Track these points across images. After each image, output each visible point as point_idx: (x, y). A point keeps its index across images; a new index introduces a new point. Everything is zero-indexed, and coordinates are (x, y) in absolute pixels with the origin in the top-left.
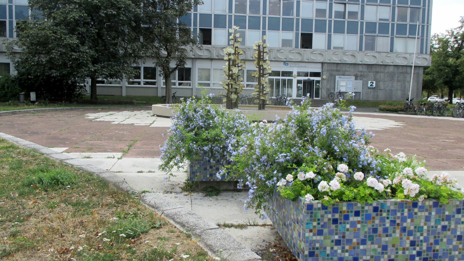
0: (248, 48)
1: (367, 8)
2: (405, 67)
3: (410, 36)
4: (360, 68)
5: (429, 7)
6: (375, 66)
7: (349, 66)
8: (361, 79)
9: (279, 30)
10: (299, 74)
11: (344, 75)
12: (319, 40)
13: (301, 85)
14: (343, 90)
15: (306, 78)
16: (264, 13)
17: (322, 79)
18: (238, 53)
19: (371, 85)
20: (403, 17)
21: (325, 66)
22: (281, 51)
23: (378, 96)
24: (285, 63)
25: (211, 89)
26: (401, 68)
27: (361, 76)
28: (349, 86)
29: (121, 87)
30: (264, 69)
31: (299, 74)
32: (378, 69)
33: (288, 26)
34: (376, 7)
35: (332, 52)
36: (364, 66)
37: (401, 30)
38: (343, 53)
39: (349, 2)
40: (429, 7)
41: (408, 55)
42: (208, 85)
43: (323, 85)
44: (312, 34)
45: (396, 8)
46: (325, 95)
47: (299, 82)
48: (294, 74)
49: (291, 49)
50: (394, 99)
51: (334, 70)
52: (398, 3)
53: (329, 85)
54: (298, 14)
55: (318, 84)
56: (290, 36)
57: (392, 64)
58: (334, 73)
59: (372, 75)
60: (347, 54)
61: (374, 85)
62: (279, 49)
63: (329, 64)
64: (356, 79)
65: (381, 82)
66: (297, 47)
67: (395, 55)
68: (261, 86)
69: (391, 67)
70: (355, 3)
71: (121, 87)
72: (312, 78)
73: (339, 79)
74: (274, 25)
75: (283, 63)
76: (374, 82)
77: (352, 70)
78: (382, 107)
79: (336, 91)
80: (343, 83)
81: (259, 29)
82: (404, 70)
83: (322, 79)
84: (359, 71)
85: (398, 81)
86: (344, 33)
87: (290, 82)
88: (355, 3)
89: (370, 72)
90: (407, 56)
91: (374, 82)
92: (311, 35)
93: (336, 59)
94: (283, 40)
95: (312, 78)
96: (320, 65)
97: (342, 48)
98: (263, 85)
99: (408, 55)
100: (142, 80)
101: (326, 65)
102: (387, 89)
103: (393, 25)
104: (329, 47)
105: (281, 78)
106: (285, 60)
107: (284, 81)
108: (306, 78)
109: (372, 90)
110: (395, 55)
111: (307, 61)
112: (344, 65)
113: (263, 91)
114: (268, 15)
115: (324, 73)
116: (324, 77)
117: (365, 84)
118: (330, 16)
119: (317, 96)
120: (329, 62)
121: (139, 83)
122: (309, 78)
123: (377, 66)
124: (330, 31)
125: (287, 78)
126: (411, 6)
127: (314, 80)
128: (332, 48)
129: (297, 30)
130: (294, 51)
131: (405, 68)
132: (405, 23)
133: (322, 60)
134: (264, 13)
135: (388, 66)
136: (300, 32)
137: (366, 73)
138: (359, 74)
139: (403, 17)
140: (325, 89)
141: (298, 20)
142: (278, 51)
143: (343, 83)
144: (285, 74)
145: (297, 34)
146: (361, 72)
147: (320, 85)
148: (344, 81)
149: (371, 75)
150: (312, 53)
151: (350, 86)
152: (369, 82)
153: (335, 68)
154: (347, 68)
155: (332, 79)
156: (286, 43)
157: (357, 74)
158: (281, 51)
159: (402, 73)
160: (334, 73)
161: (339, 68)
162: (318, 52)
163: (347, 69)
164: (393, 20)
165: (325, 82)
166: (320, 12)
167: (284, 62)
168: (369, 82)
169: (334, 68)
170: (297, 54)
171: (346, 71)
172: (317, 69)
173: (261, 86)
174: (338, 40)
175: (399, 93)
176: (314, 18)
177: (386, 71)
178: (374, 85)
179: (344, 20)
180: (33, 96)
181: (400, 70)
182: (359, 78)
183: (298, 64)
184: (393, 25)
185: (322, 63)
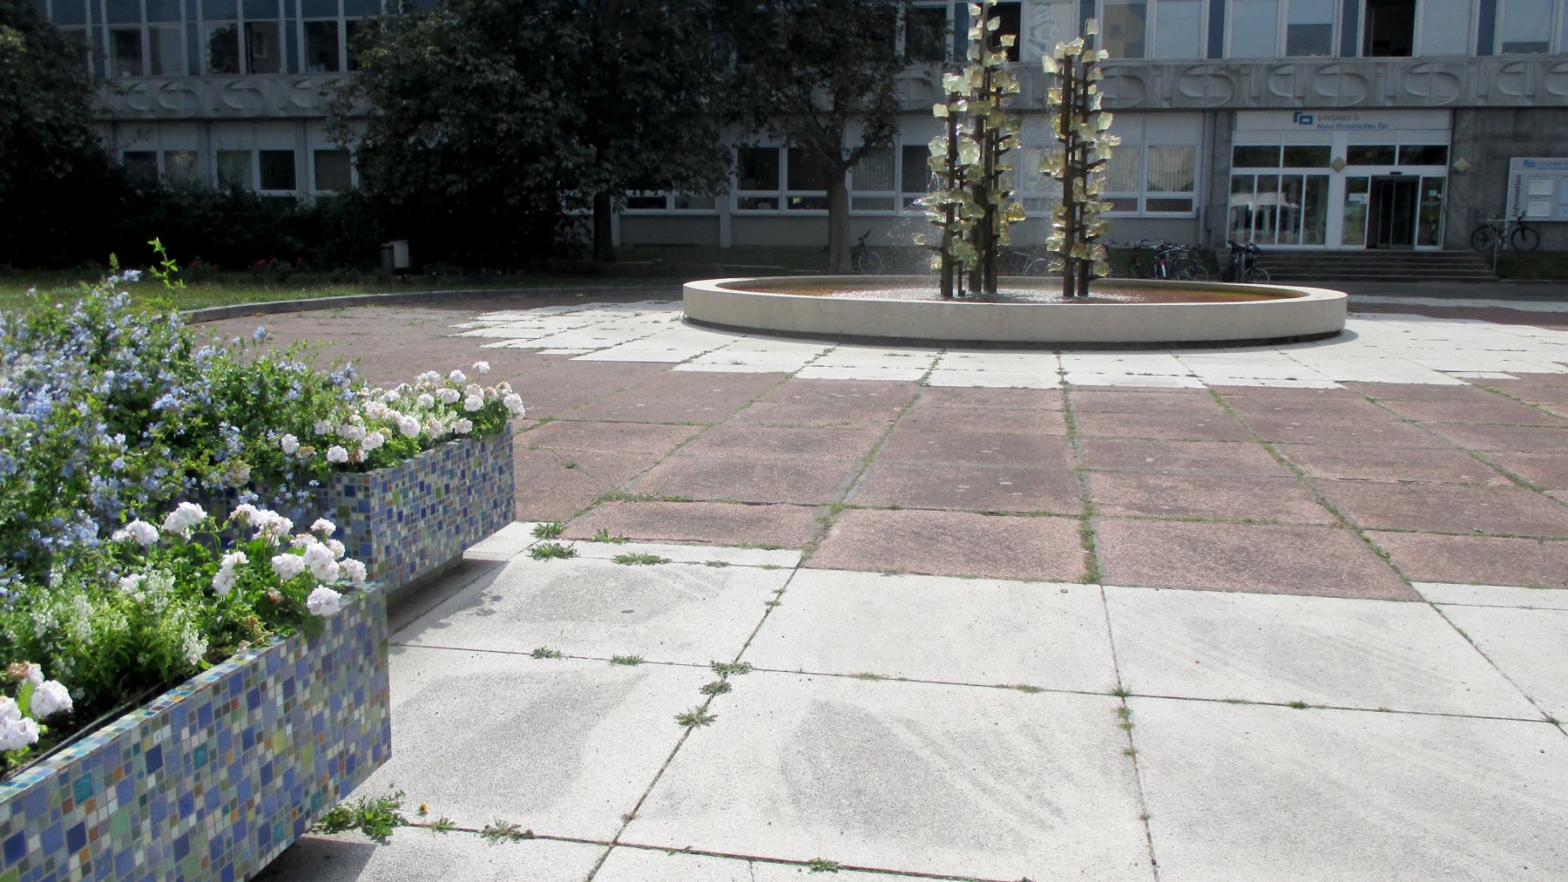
0: (1157, 67)
10: (1357, 155)
13: (1365, 198)
15: (1383, 171)
17: (1453, 172)
18: (999, 90)
21: (1466, 121)
22: (1284, 71)
24: (1301, 113)
29: (717, 218)
30: (1086, 148)
31: (1357, 155)
47: (1354, 185)
48: (1333, 157)
49: (1323, 59)
55: (1433, 193)
62: (1275, 63)
66: (1348, 50)
72: (1408, 170)
73: (1525, 172)
75: (1291, 115)
79: (1510, 216)
80: (1536, 188)
87: (1318, 188)
93: (1511, 92)
95: (1408, 170)
96: (1444, 120)
97: (1542, 47)
100: (783, 192)
101: (1472, 114)
104: (1485, 47)
106: (1298, 104)
108: (1383, 171)
111: (1389, 104)
113: (1083, 229)
116: (1461, 164)
120: (1481, 103)
121: (774, 203)
122: (1396, 168)
128: (1498, 50)
140: (1465, 211)
142: (1272, 69)
143: (1536, 188)
144: (1298, 156)
147: (1443, 196)
148: (1547, 177)
150: (1409, 71)
155: (1494, 167)
158: (1284, 71)
162: (1438, 69)
167: (1297, 111)
169: (1506, 126)
172: (1434, 132)
179: (351, 18)
180: (400, 253)
185: (1456, 111)
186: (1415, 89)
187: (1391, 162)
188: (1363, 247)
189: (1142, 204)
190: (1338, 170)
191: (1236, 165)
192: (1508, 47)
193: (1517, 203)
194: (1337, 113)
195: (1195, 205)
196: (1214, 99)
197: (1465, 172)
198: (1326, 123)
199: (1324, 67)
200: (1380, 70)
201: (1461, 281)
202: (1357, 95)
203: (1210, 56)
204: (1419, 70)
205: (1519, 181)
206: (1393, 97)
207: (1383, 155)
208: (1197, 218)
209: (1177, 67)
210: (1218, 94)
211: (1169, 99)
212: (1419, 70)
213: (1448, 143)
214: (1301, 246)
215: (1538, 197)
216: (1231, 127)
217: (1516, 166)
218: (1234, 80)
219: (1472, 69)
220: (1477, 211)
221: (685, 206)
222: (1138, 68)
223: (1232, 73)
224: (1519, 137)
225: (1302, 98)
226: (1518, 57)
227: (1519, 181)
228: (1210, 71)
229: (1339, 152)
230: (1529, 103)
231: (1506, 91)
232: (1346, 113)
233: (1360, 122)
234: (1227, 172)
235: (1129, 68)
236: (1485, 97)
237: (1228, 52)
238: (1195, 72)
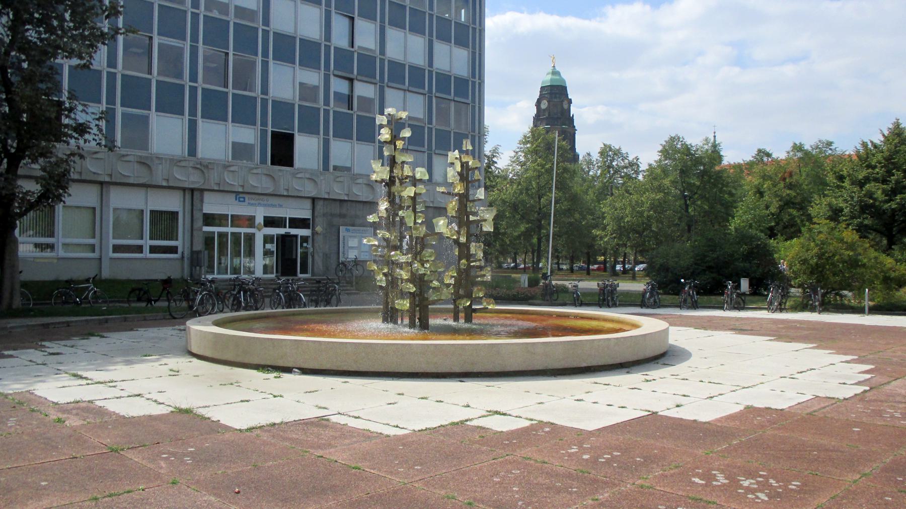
5: (479, 104)
9: (226, 120)
10: (270, 222)
11: (353, 225)
13: (272, 247)
16: (194, 78)
20: (443, 115)
21: (319, 205)
22: (232, 169)
24: (240, 195)
25: (59, 259)
31: (270, 222)
33: (244, 115)
34: (401, 93)
39: (359, 78)
40: (479, 104)
42: (51, 247)
43: (316, 245)
45: (434, 100)
47: (267, 239)
49: (250, 164)
52: (437, 91)
54: (265, 90)
55: (305, 245)
56: (247, 135)
60: (359, 181)
66: (263, 161)
70: (369, 80)
72: (294, 231)
73: (346, 234)
74: (214, 108)
75: (234, 195)
80: (353, 243)
81: (182, 114)
86: (352, 139)
87: (250, 238)
88: (369, 80)
92: (290, 138)
93: (339, 191)
94: (234, 144)
95: (294, 231)
96: (308, 204)
97: (348, 169)
103: (430, 129)
105: (229, 230)
106: (240, 190)
107: (236, 236)
108: (282, 231)
114: (201, 84)
115: (317, 220)
118: (327, 103)
119: (304, 270)
120: (326, 197)
124: (326, 132)
125: (243, 230)
126: (456, 99)
127: (296, 236)
129: (264, 123)
130: (259, 171)
132: (447, 129)
133: (312, 194)
134: (194, 78)
140: (321, 255)
141: (264, 102)
142: (226, 167)
144: (236, 220)
145: (264, 133)
148: (355, 237)
150: (294, 175)
153: (337, 211)
156: (240, 150)
158: (232, 169)
162: (308, 176)
165: (319, 239)
166: (307, 91)
167: (237, 193)
169: (336, 209)
170: (264, 178)
172: (304, 213)
174: (341, 151)
176: (297, 102)
184: (430, 129)
185: (314, 200)
187: (285, 227)
188: (273, 276)
189: (146, 249)
192: (336, 168)
194: (257, 197)
195: (180, 250)
196: (193, 182)
199: (252, 169)
202: (265, 185)
203: (189, 155)
204: (299, 176)
208: (183, 257)
209: (171, 160)
210: (193, 180)
211: (168, 180)
212: (299, 176)
213: (310, 217)
214: (229, 276)
215: (352, 248)
218: (205, 171)
222: (147, 158)
223: (204, 167)
224: (342, 216)
226: (338, 173)
228: (191, 165)
229: (260, 220)
230: (346, 198)
232: (261, 197)
233: (269, 203)
234: (201, 229)
235: (141, 157)
236: (329, 193)
237: (201, 153)
238: (183, 164)
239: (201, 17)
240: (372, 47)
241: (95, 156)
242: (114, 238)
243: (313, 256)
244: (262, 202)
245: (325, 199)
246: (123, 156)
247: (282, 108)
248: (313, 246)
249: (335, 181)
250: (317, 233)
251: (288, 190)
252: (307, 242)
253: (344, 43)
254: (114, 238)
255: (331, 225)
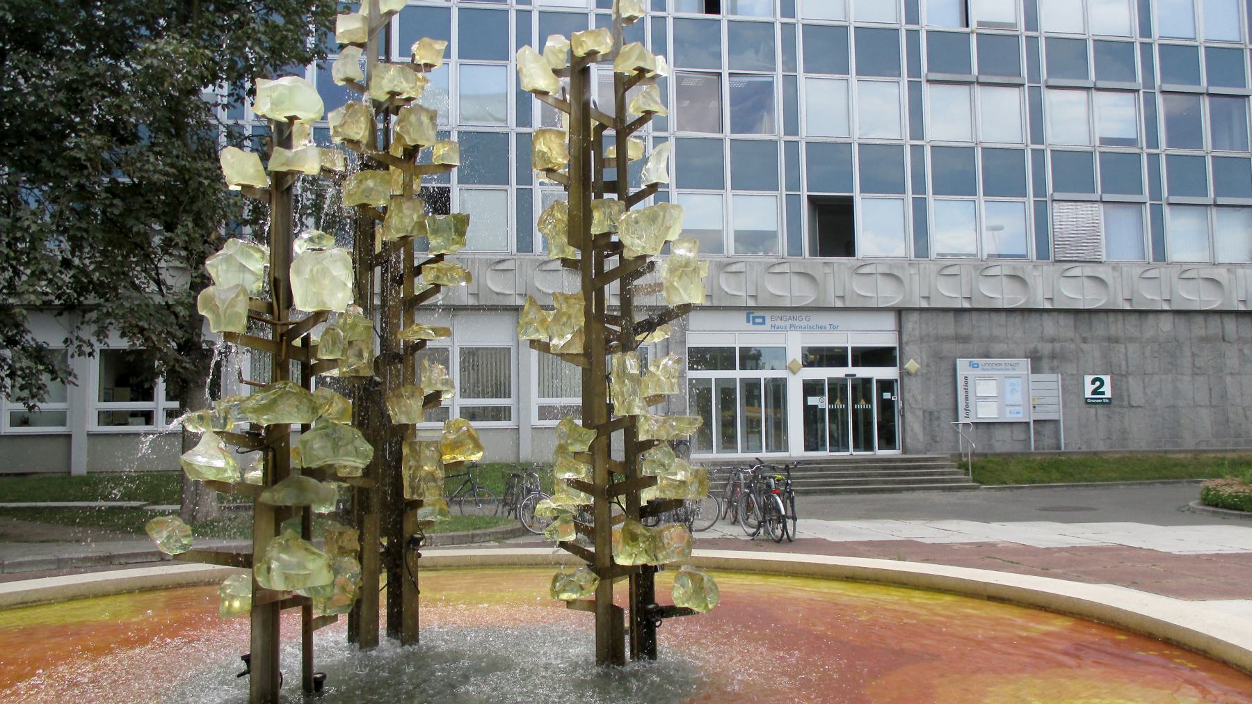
1: (1051, 99)
2: (1217, 318)
3: (1220, 201)
4: (1049, 326)
6: (1102, 316)
7: (1002, 318)
8: (1053, 370)
11: (987, 357)
12: (878, 225)
14: (987, 412)
15: (838, 372)
17: (904, 374)
19: (1094, 392)
20: (1183, 130)
21: (911, 322)
22: (734, 268)
23: (1124, 432)
24: (755, 312)
26: (1200, 320)
27: (1053, 356)
28: (1010, 399)
32: (1117, 327)
33: (755, 172)
34: (1082, 95)
35: (934, 268)
36: (1063, 320)
37: (1186, 177)
38: (976, 267)
41: (1223, 271)
43: (907, 395)
44: (851, 199)
45: (1160, 99)
46: (921, 436)
47: (811, 388)
50: (1189, 442)
51: (946, 339)
52: (1163, 80)
53: (932, 397)
54: (792, 125)
55: (887, 396)
57: (1166, 307)
58: (947, 348)
59: (1097, 354)
61: (1107, 390)
63: (925, 316)
64: (1036, 369)
65: (1130, 379)
66: (795, 249)
67: (1175, 271)
68: (618, 438)
69: (1163, 317)
71: (68, 437)
73: (971, 373)
75: (743, 315)
76: (1107, 379)
77: (1019, 334)
78: (1228, 487)
80: (985, 388)
82: (1214, 325)
83: (904, 374)
84: (1042, 339)
85: (1196, 372)
87: (778, 390)
89: (1085, 340)
90: (1221, 274)
91: (1107, 379)
93: (949, 294)
95: (863, 372)
96: (889, 322)
98: (630, 425)
99: (1223, 271)
101: (914, 317)
102: (1158, 402)
105: (738, 374)
106: (751, 303)
109: (1101, 411)
110: (1175, 271)
111: (839, 304)
112: (986, 316)
115: (907, 349)
116: (911, 365)
117: (1071, 388)
119: (888, 439)
120: (924, 304)
122: (850, 370)
123: (1111, 318)
124: (919, 186)
126: (1213, 90)
129: (793, 184)
130: (785, 268)
131: (1215, 322)
133: (896, 302)
135: (1151, 316)
136: (804, 193)
137: (1073, 346)
138: (1046, 348)
139: (1183, 130)
140: (920, 413)
141: (792, 147)
143: (985, 388)
144: (751, 358)
145: (793, 201)
146: (1053, 340)
148: (990, 378)
149: (1093, 351)
150: (856, 271)
151: (1017, 398)
152: (1088, 379)
154: (997, 327)
157: (1036, 351)
158: (734, 268)
159: (1205, 339)
160: (947, 348)
161: (965, 330)
162: (882, 269)
163: (998, 332)
164: (1153, 141)
168: (1088, 379)
169: (947, 326)
170: (795, 279)
171: (993, 339)
172: (881, 335)
173: (618, 438)
175: (1206, 416)
177: (1149, 333)
178: (1107, 390)
181: (1199, 328)
182: (1045, 364)
183: (803, 320)
184: (1154, 158)
185: (900, 312)
186: (862, 290)
187: (845, 365)
190: (794, 373)
191: (691, 368)
193: (967, 405)
194: (789, 314)
197: (916, 374)
198: (779, 323)
200: (827, 270)
201: (943, 489)
202: (803, 293)
205: (966, 383)
206: (842, 298)
207: (834, 357)
215: (985, 398)
216: (684, 329)
217: (962, 364)
219: (912, 271)
220: (931, 413)
221: (25, 422)
224: (960, 339)
225: (755, 297)
227: (966, 383)
230: (966, 305)
231: (946, 293)
232: (796, 314)
233: (810, 323)
239: (670, 23)
240: (1009, 18)
241: (500, 267)
242: (542, 394)
243: (903, 416)
244: (797, 323)
245: (921, 310)
246: (546, 262)
247: (828, 154)
248: (903, 400)
249: (940, 273)
250: (909, 374)
251: (842, 298)
252: (891, 391)
253: (949, 22)
254: (542, 394)
255: (938, 357)
